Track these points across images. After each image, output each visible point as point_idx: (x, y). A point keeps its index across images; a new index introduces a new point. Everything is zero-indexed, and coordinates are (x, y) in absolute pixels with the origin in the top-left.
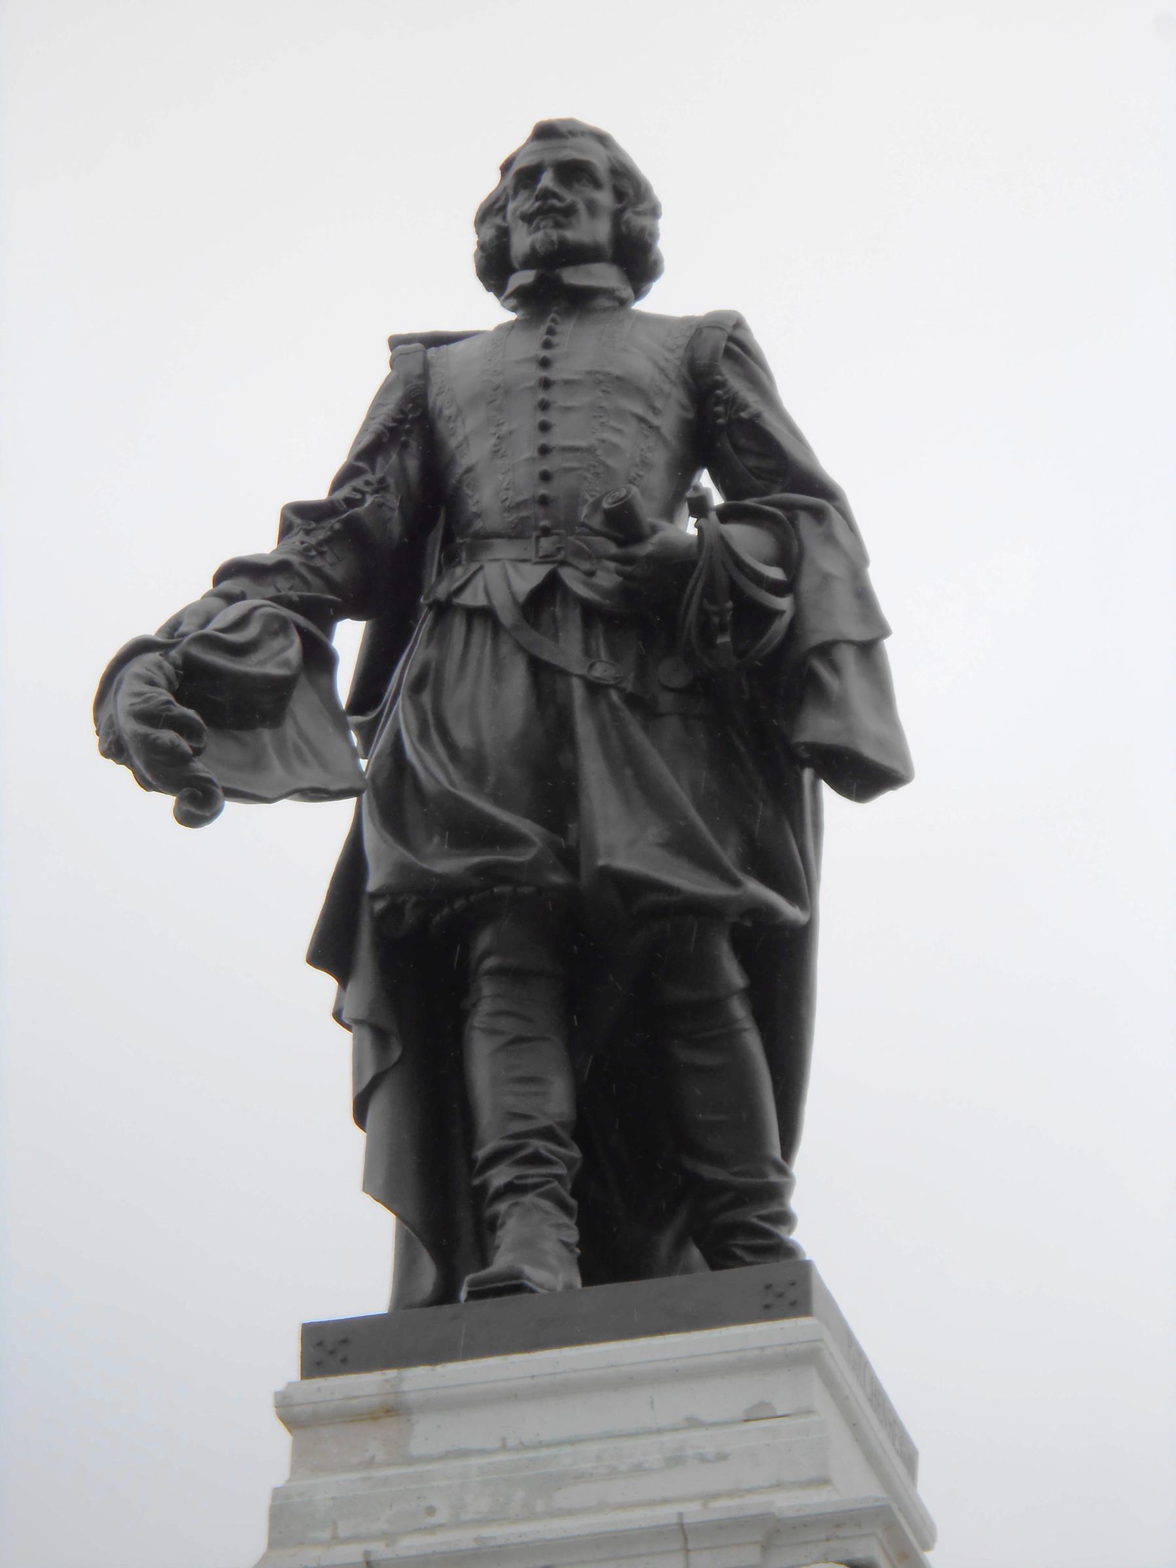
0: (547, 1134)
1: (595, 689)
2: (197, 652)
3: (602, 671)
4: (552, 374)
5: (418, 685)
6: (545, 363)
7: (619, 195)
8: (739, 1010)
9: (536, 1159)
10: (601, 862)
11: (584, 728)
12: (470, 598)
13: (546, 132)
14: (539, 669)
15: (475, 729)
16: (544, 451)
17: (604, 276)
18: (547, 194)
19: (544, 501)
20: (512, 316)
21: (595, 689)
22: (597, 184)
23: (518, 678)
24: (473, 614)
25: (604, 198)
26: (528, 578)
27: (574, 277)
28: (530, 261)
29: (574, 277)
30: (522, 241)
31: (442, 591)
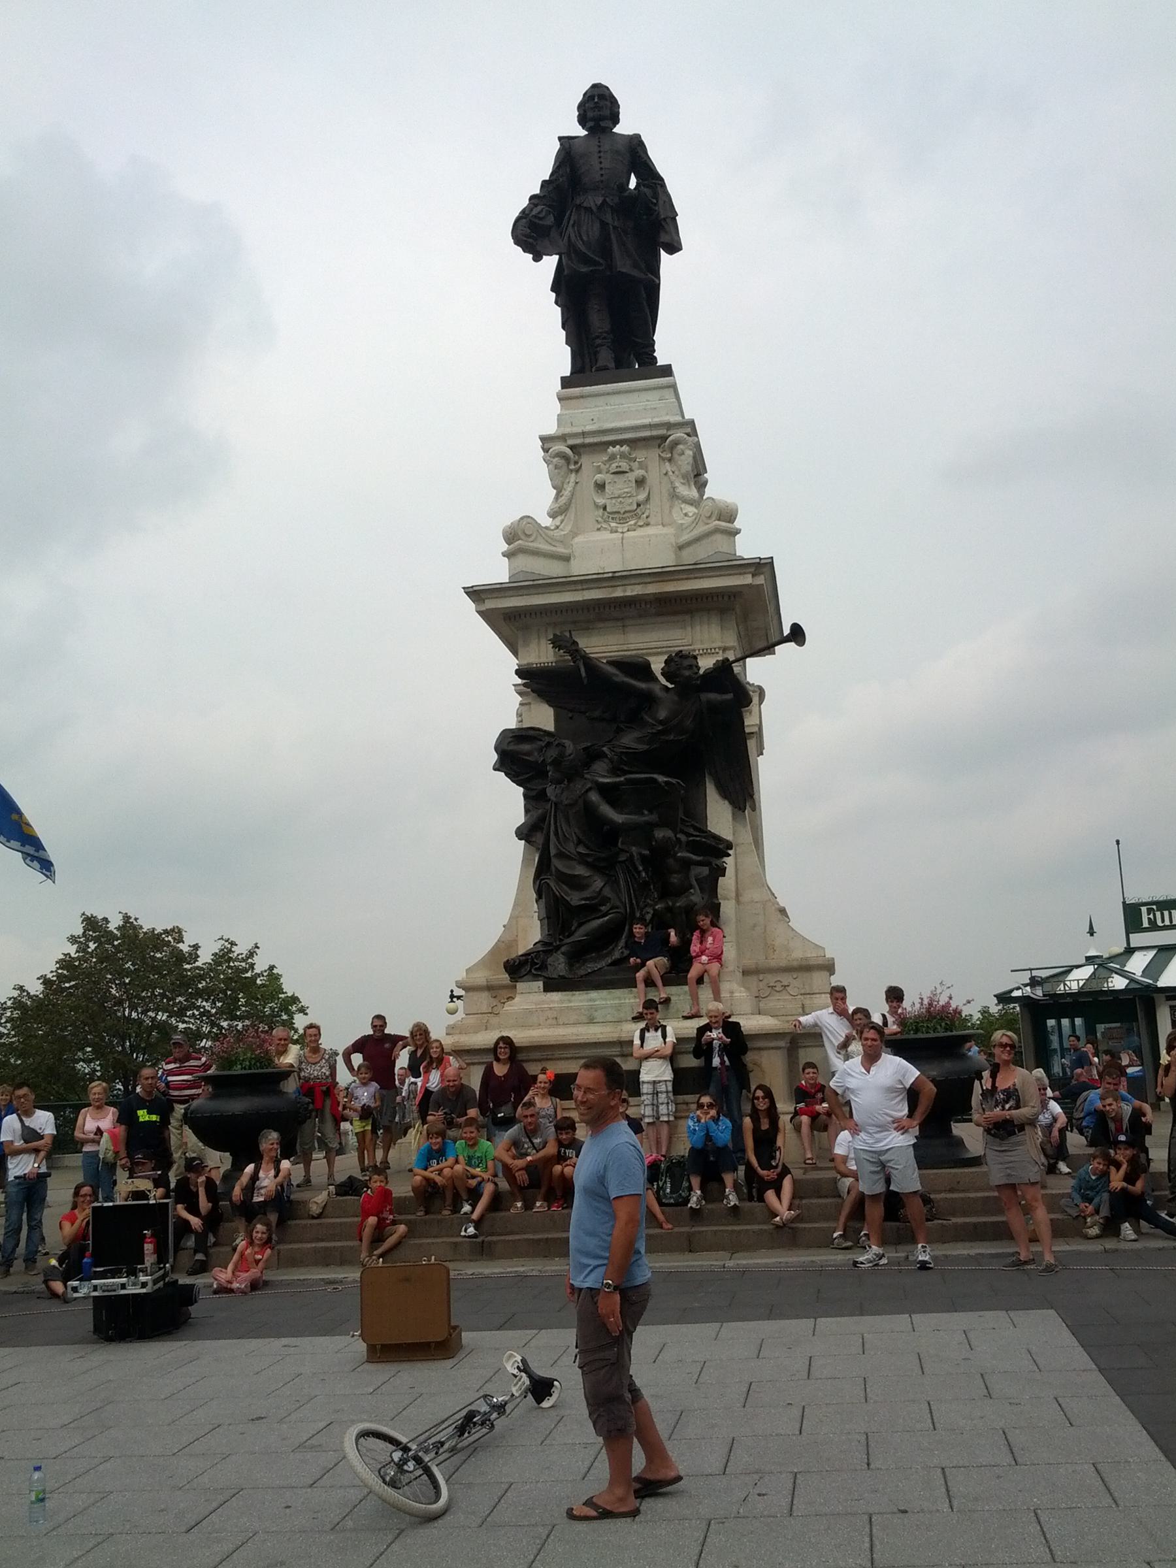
0: (606, 332)
1: (615, 228)
2: (534, 220)
3: (616, 224)
4: (602, 149)
5: (573, 226)
6: (599, 146)
7: (612, 103)
8: (645, 303)
9: (604, 338)
10: (618, 270)
11: (613, 237)
12: (585, 205)
13: (594, 86)
14: (604, 225)
15: (588, 236)
16: (601, 169)
17: (609, 123)
18: (596, 103)
19: (602, 181)
20: (587, 133)
21: (615, 228)
22: (606, 100)
23: (597, 226)
24: (586, 208)
25: (608, 104)
26: (599, 201)
27: (603, 124)
28: (592, 119)
29: (603, 124)
30: (590, 114)
31: (578, 202)
